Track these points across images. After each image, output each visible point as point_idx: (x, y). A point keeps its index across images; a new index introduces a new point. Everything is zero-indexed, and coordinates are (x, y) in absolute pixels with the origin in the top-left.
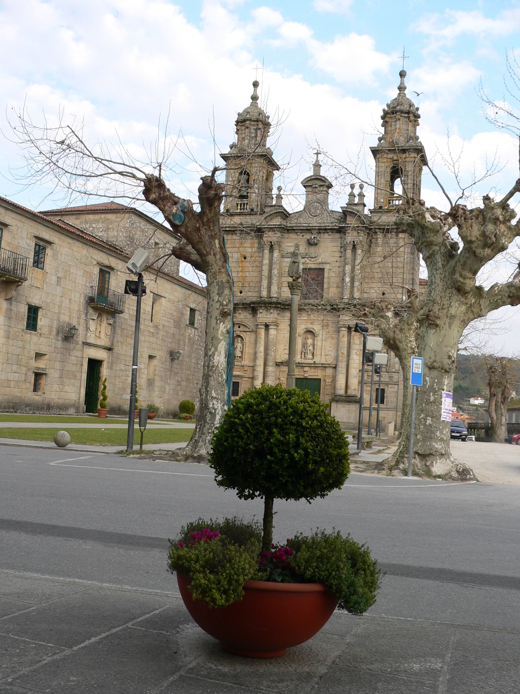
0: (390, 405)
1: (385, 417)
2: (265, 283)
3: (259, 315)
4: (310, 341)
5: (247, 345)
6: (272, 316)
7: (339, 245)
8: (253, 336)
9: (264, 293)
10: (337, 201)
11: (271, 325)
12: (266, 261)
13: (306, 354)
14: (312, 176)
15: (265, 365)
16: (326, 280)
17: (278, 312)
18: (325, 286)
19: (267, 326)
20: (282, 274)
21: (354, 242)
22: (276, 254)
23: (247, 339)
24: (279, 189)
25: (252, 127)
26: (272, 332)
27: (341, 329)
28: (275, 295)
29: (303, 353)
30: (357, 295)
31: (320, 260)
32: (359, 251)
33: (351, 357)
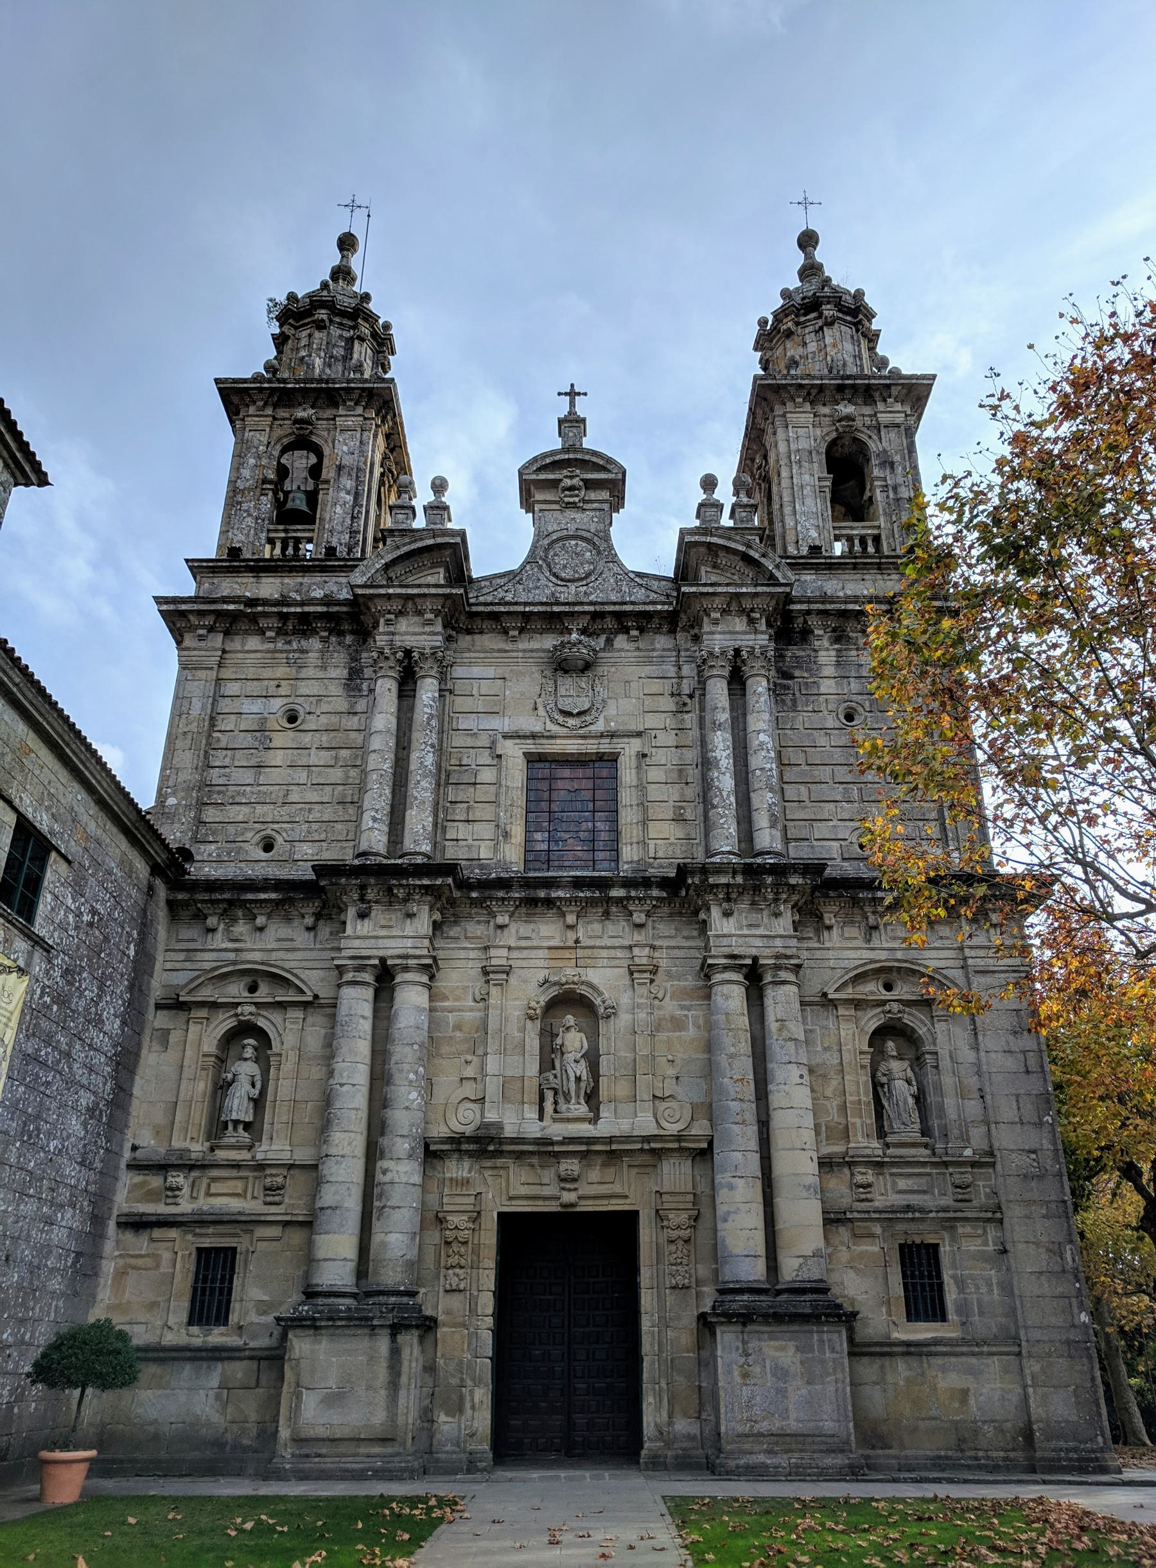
0: (983, 1326)
1: (965, 1393)
2: (378, 798)
3: (356, 927)
4: (574, 1041)
5: (288, 1066)
6: (410, 928)
7: (672, 671)
8: (315, 1030)
9: (375, 838)
10: (646, 542)
11: (406, 969)
12: (385, 719)
13: (561, 1100)
14: (553, 453)
15: (373, 1153)
16: (627, 797)
17: (437, 916)
18: (628, 817)
19: (385, 978)
20: (448, 776)
21: (737, 651)
22: (427, 691)
23: (290, 1039)
24: (439, 486)
25: (335, 332)
26: (411, 998)
27: (717, 977)
28: (426, 847)
29: (549, 1095)
30: (767, 838)
31: (600, 726)
32: (759, 687)
33: (776, 1099)
